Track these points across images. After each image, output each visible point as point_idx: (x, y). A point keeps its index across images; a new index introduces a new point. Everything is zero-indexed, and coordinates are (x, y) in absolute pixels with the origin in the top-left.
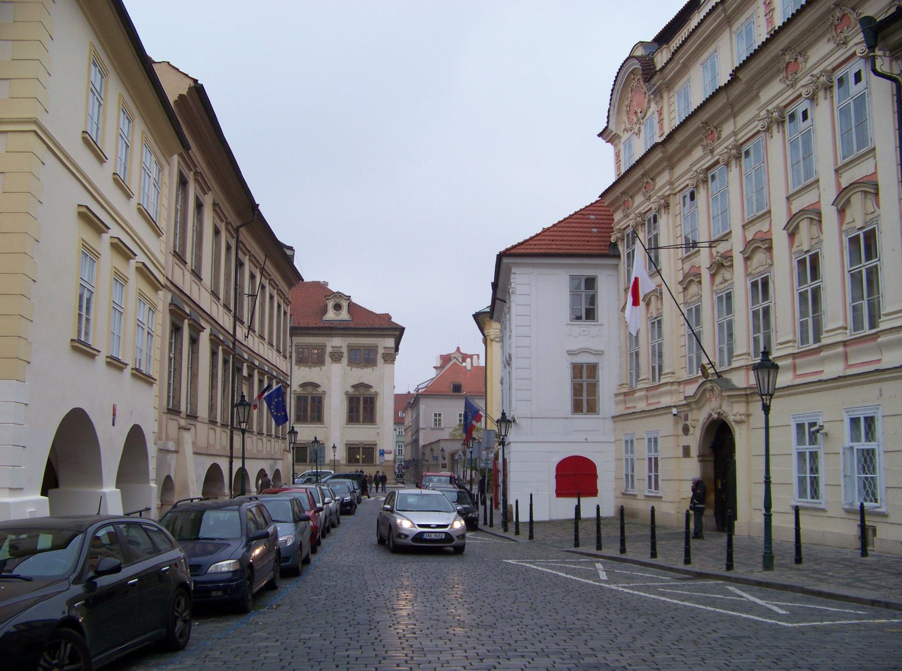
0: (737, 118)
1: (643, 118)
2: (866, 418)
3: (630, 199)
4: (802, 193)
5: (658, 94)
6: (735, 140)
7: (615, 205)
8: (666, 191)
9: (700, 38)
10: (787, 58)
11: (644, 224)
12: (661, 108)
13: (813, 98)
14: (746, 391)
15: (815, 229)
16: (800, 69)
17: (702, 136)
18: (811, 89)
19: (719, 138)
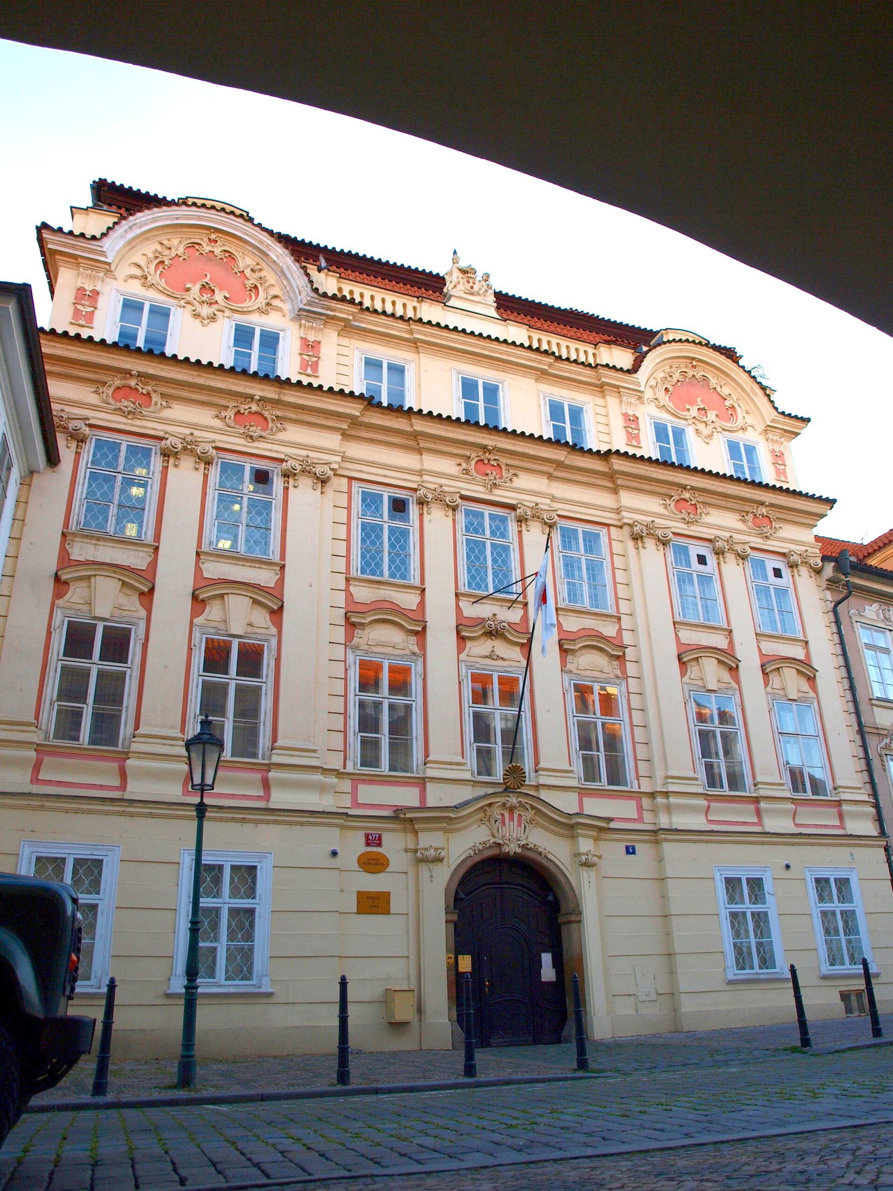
9: (482, 349)
10: (686, 495)
14: (608, 823)
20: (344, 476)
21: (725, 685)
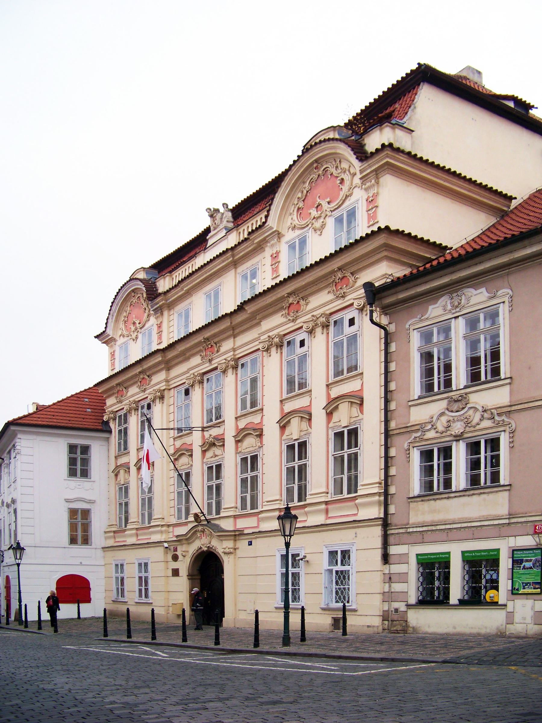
0: (237, 339)
1: (141, 328)
2: (342, 552)
3: (124, 389)
4: (294, 399)
5: (159, 311)
6: (233, 355)
7: (109, 392)
8: (163, 386)
10: (291, 300)
11: (138, 409)
12: (161, 322)
13: (311, 332)
15: (305, 425)
16: (301, 310)
17: (202, 348)
18: (311, 325)
19: (218, 351)
20: (172, 388)
21: (305, 433)
